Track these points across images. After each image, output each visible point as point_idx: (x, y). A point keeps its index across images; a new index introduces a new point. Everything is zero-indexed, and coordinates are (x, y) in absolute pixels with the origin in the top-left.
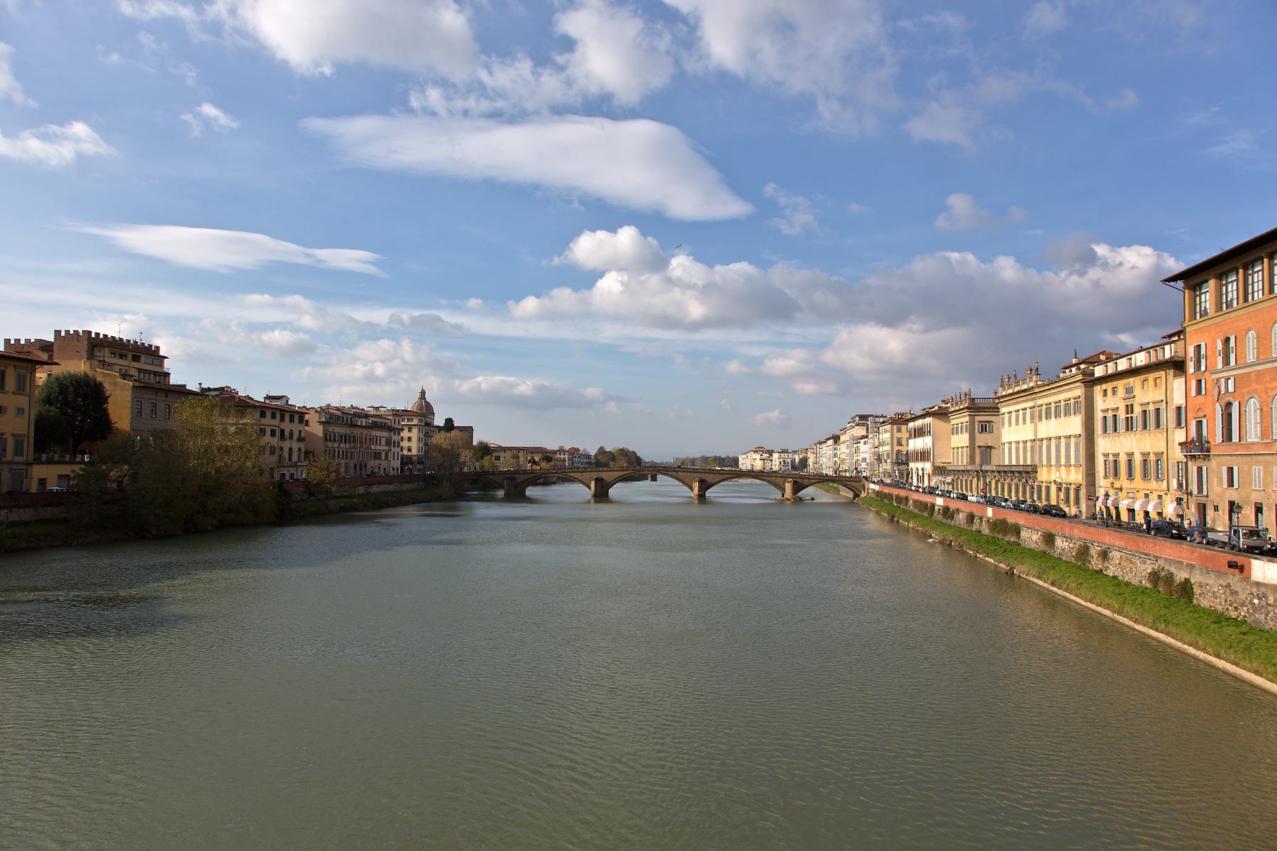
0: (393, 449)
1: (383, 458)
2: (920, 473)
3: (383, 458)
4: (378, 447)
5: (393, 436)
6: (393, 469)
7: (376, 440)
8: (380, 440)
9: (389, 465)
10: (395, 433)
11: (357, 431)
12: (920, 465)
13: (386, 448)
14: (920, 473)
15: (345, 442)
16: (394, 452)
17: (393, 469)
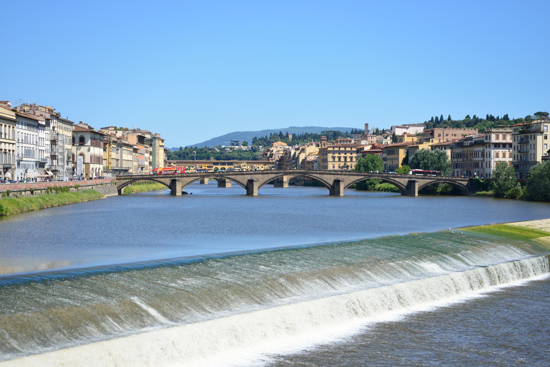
0: (486, 159)
1: (480, 166)
2: (97, 171)
3: (480, 166)
4: (477, 159)
5: (485, 149)
6: (487, 174)
7: (476, 154)
8: (478, 153)
9: (484, 172)
10: (486, 147)
11: (466, 149)
12: (97, 166)
13: (482, 159)
14: (97, 171)
15: (460, 158)
16: (487, 162)
17: (487, 174)
